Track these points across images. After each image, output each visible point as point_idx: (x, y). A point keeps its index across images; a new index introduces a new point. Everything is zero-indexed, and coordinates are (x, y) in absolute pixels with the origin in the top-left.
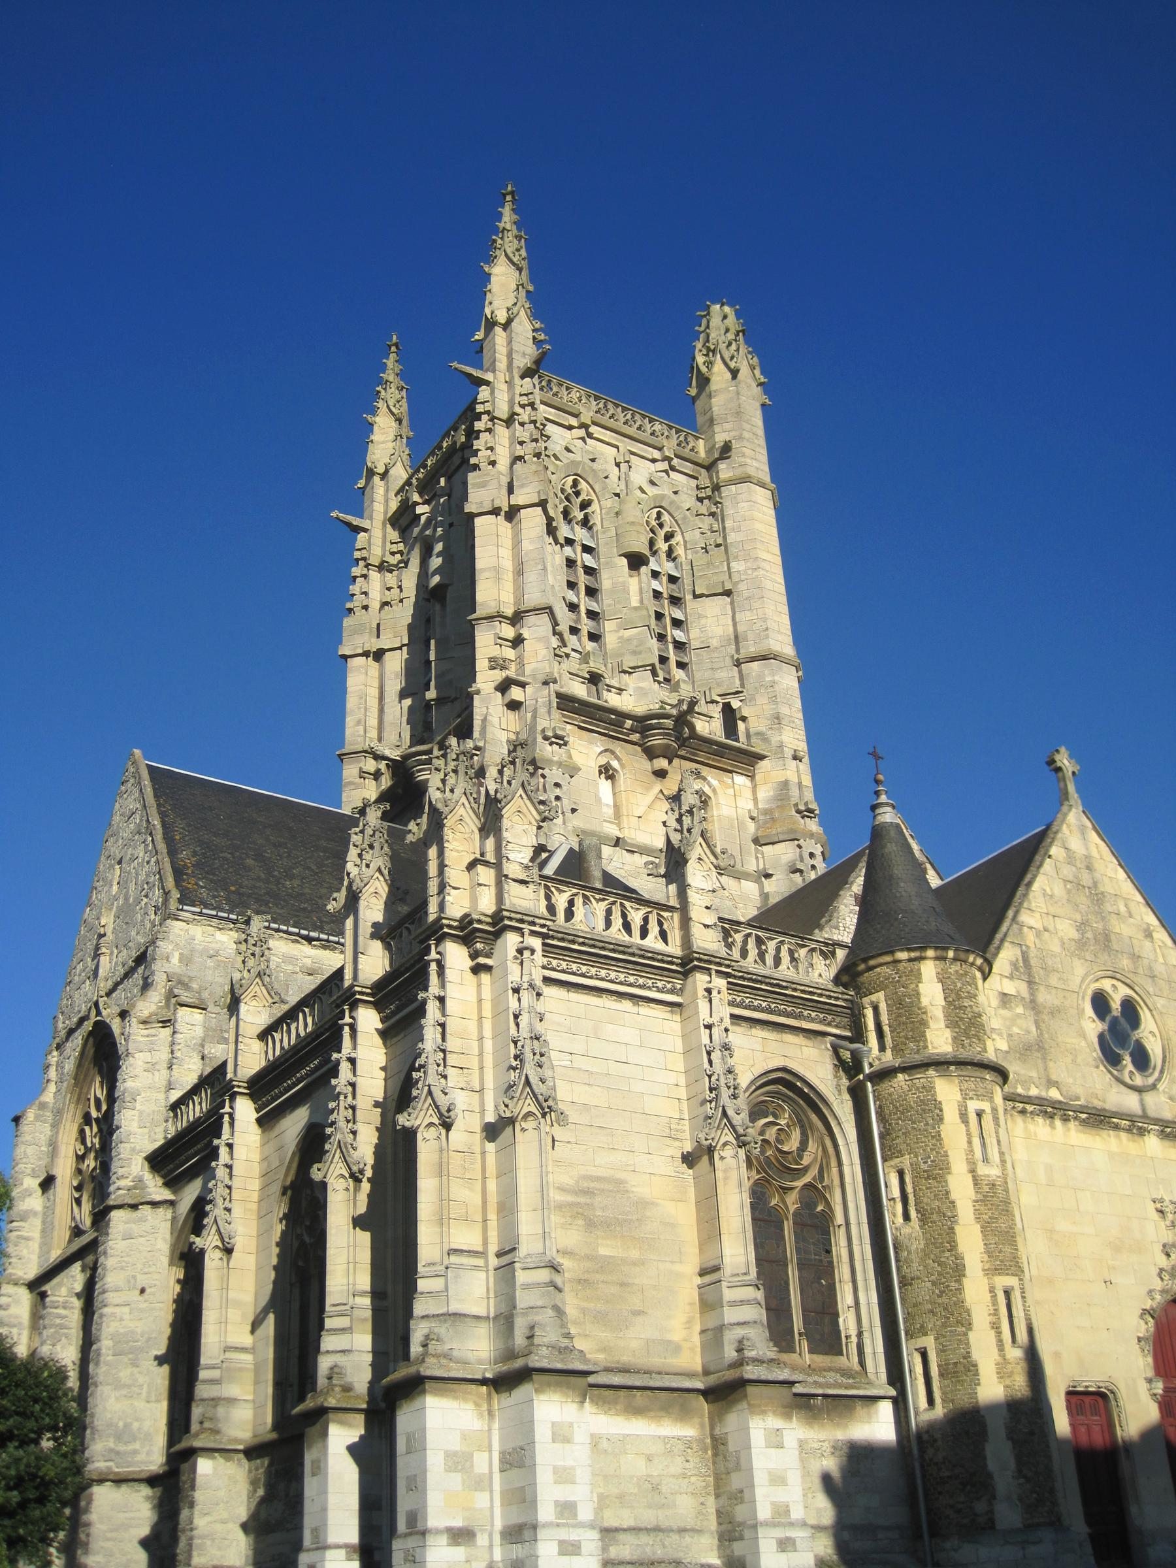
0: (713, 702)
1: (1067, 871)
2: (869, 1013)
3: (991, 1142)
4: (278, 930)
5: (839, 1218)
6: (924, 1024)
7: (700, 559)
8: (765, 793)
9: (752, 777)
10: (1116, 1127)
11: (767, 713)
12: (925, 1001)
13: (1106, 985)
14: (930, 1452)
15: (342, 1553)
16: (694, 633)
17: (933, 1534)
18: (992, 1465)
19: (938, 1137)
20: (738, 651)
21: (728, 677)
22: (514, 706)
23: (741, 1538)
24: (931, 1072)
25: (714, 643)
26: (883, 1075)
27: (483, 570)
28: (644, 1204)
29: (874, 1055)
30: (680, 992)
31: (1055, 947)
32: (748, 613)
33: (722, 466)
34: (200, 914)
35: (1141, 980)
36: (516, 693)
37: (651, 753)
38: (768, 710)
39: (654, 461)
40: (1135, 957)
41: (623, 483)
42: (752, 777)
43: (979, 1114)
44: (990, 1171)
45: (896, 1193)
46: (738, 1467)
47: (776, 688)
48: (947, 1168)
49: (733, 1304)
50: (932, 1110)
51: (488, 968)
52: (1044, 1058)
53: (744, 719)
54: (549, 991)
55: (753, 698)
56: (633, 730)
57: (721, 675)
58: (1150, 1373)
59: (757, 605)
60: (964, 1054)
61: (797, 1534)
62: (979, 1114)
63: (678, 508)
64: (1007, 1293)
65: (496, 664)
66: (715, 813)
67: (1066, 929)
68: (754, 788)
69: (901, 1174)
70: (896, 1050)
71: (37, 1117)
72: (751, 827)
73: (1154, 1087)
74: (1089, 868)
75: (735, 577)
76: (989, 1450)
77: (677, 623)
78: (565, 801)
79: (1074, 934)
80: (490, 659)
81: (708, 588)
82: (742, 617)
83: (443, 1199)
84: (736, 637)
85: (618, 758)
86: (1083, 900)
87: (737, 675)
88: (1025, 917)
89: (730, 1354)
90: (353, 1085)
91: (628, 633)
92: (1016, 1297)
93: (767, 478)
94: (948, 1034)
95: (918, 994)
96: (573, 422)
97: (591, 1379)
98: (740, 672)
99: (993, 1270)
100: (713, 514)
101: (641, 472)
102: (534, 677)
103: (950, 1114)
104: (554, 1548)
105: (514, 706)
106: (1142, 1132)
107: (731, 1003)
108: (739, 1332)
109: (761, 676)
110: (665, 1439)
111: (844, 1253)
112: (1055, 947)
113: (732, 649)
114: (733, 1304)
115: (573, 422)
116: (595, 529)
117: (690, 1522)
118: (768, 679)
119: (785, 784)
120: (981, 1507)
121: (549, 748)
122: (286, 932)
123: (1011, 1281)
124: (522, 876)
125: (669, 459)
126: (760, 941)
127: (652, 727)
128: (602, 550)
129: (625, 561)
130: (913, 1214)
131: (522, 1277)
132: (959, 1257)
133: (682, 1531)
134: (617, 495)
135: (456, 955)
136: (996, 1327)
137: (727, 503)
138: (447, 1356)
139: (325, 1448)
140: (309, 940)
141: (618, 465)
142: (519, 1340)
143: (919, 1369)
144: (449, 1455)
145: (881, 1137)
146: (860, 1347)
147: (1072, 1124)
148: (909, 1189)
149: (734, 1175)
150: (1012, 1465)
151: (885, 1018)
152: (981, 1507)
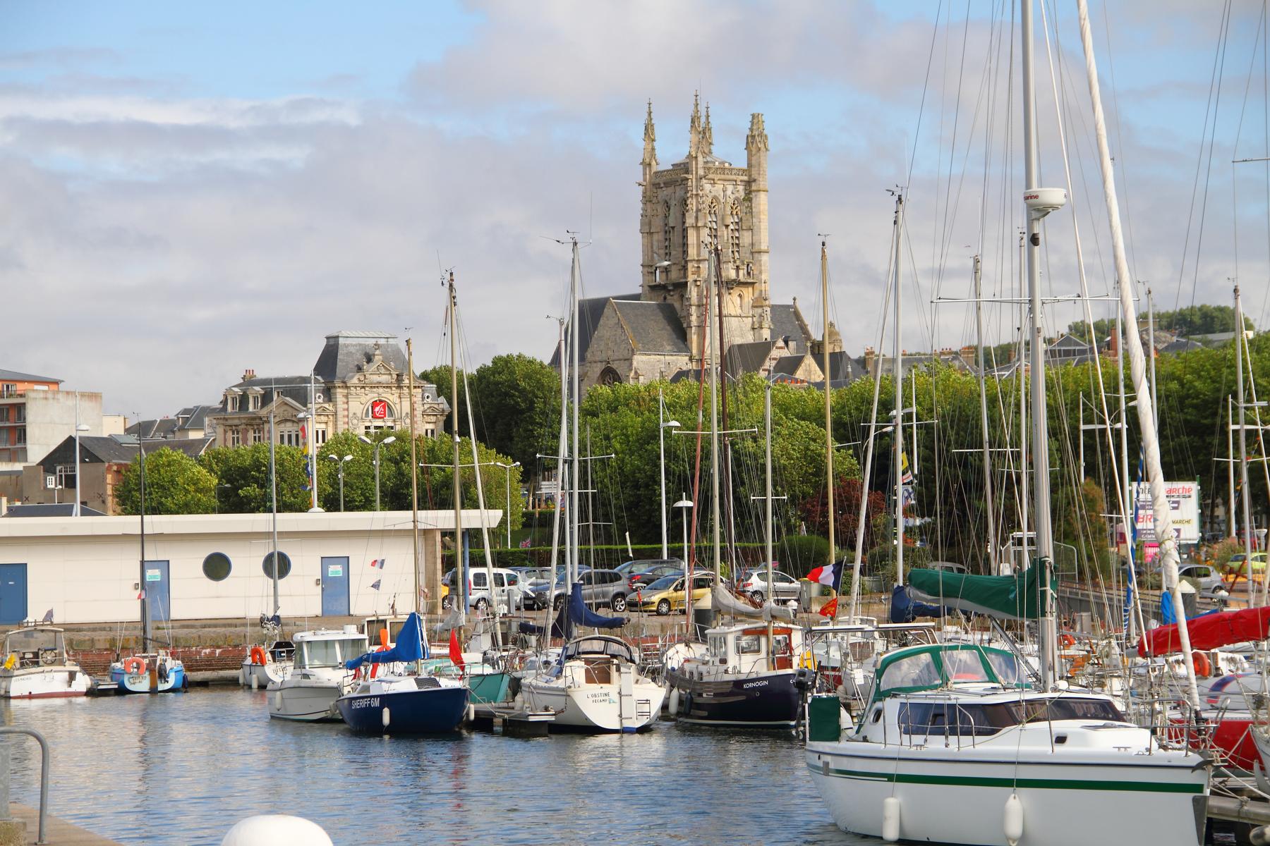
25: (746, 245)
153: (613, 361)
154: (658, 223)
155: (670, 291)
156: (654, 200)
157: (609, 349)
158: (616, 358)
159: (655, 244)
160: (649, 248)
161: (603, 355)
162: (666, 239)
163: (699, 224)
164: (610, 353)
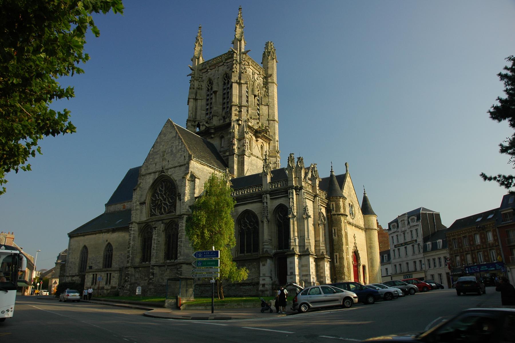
2: (331, 205)
6: (340, 208)
12: (340, 205)
15: (269, 277)
20: (269, 117)
23: (323, 278)
27: (234, 95)
34: (196, 160)
41: (254, 78)
75: (270, 103)
77: (258, 109)
80: (235, 114)
84: (268, 115)
90: (267, 207)
91: (253, 111)
93: (276, 83)
98: (269, 122)
103: (343, 222)
108: (323, 250)
109: (273, 124)
130: (336, 236)
136: (346, 253)
140: (210, 167)
148: (336, 232)
153: (168, 169)
155: (212, 133)
157: (164, 159)
158: (170, 166)
159: (199, 108)
160: (194, 110)
162: (207, 104)
163: (242, 82)
164: (165, 163)
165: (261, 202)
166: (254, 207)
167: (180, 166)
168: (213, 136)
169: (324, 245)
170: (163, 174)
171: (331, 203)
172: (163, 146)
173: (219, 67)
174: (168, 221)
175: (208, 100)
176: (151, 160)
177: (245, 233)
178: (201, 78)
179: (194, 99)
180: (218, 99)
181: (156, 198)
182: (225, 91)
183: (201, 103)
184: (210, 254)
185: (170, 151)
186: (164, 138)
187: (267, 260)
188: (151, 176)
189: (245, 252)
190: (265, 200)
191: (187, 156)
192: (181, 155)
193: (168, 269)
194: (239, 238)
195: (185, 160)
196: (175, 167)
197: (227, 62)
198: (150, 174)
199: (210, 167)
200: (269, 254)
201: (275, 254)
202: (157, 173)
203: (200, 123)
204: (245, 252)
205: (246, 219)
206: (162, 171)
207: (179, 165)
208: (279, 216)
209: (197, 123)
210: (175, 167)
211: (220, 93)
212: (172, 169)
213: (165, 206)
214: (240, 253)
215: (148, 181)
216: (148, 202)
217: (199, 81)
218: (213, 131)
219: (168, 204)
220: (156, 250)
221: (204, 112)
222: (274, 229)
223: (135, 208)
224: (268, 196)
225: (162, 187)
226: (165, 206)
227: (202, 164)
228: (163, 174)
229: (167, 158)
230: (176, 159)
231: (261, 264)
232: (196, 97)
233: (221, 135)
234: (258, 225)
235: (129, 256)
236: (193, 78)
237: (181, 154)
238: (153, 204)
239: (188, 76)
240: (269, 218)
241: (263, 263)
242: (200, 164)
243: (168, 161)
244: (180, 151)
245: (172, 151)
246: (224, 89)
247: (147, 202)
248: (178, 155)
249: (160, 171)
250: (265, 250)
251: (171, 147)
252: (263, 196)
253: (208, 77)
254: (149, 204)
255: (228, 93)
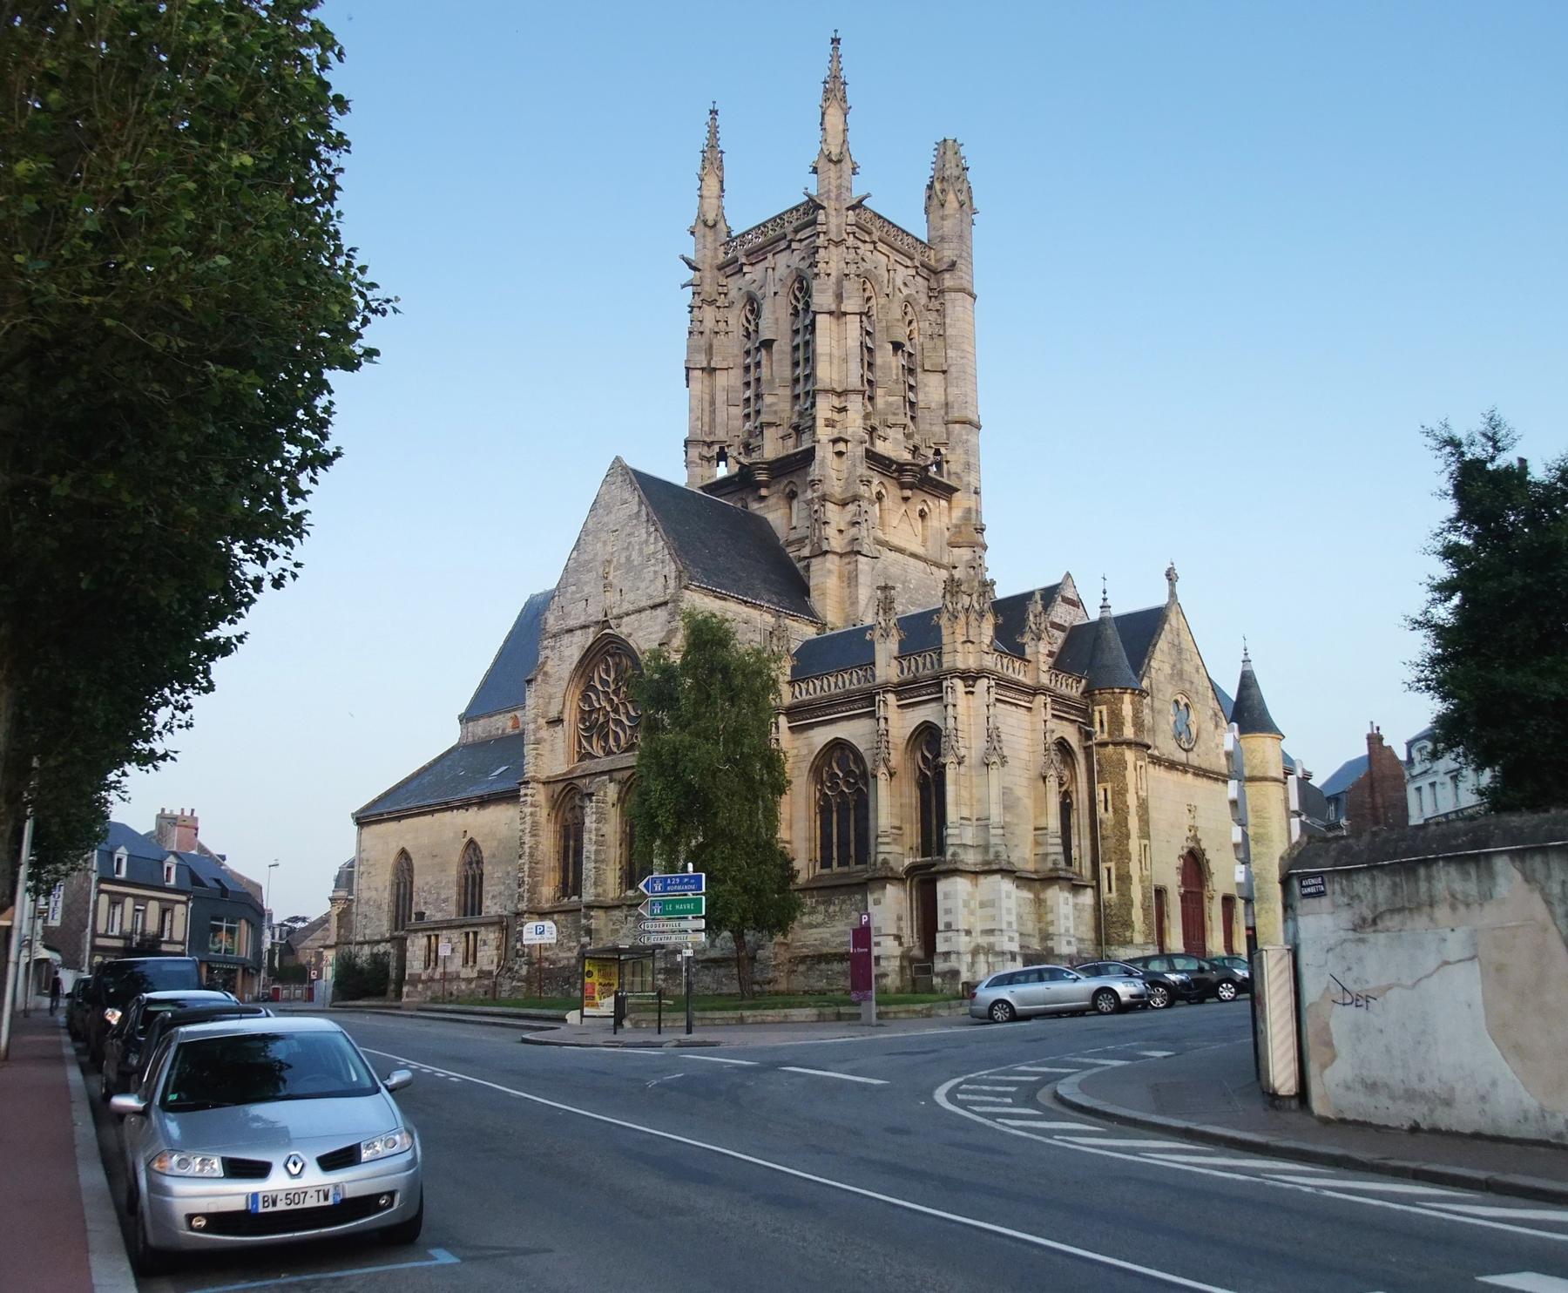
0: (930, 447)
1: (1170, 637)
3: (1144, 780)
4: (733, 597)
5: (1075, 807)
6: (1123, 724)
7: (928, 344)
8: (957, 514)
9: (949, 501)
10: (1178, 770)
11: (962, 461)
12: (1124, 713)
13: (1179, 697)
14: (1108, 911)
15: (892, 938)
16: (921, 396)
17: (1107, 944)
18: (1134, 918)
19: (1124, 776)
20: (946, 413)
21: (939, 429)
22: (840, 454)
23: (1052, 939)
24: (1124, 747)
25: (933, 405)
26: (1104, 744)
28: (1019, 799)
29: (1101, 735)
30: (1030, 702)
31: (1162, 679)
32: (955, 389)
33: (947, 275)
34: (699, 587)
35: (1191, 694)
36: (841, 447)
37: (903, 486)
38: (963, 458)
39: (907, 267)
40: (1192, 683)
41: (891, 285)
42: (949, 501)
43: (1141, 767)
44: (1143, 794)
45: (1103, 798)
46: (1052, 912)
47: (969, 444)
48: (1127, 791)
49: (1052, 845)
50: (1122, 764)
51: (972, 693)
52: (1154, 735)
53: (947, 462)
54: (998, 704)
55: (954, 449)
56: (895, 471)
57: (936, 429)
58: (1180, 883)
59: (962, 384)
60: (1138, 740)
61: (1072, 939)
62: (1141, 767)
63: (918, 303)
64: (1145, 846)
65: (830, 423)
66: (929, 524)
67: (1167, 669)
68: (950, 508)
69: (1105, 790)
70: (1110, 734)
71: (542, 681)
72: (947, 534)
73: (1192, 749)
74: (1178, 635)
75: (949, 361)
76: (1134, 912)
77: (911, 387)
78: (870, 522)
79: (1170, 672)
80: (826, 419)
81: (932, 366)
82: (952, 390)
83: (958, 795)
85: (885, 488)
86: (1174, 652)
87: (944, 430)
88: (1152, 663)
89: (1050, 865)
90: (887, 731)
91: (891, 399)
92: (1148, 848)
94: (1132, 730)
95: (1121, 709)
96: (867, 238)
97: (1017, 874)
98: (947, 429)
99: (1141, 837)
100: (937, 311)
101: (902, 274)
102: (853, 436)
103: (1130, 766)
104: (942, 940)
105: (840, 454)
106: (1186, 772)
107: (1053, 709)
108: (1054, 857)
110: (1024, 899)
111: (1076, 821)
112: (1162, 679)
113: (943, 412)
114: (1052, 845)
115: (867, 238)
116: (873, 318)
117: (1031, 932)
118: (965, 437)
119: (969, 510)
120: (1128, 934)
121: (862, 487)
122: (737, 598)
123: (1146, 842)
124: (986, 650)
125: (916, 267)
126: (1057, 676)
127: (907, 470)
128: (877, 335)
129: (891, 347)
130: (1110, 808)
131: (993, 831)
132: (1128, 830)
133: (1029, 935)
134: (888, 295)
135: (959, 684)
137: (948, 305)
138: (962, 861)
139: (884, 895)
140: (746, 602)
141: (889, 271)
142: (991, 857)
143: (1106, 875)
144: (964, 901)
145: (1098, 772)
146: (1080, 863)
147: (1162, 768)
148: (1109, 797)
149: (1053, 789)
150: (1142, 919)
151: (1105, 718)
152: (1128, 934)
153: (620, 617)
154: (731, 348)
155: (761, 485)
156: (721, 301)
157: (607, 587)
158: (626, 607)
159: (721, 398)
160: (706, 405)
161: (590, 610)
162: (747, 384)
164: (612, 597)
165: (872, 714)
166: (854, 731)
167: (654, 607)
168: (764, 492)
169: (1059, 841)
170: (607, 631)
171: (1096, 708)
172: (605, 543)
173: (776, 256)
174: (627, 773)
175: (747, 369)
176: (574, 588)
177: (834, 809)
178: (723, 296)
179: (703, 369)
180: (777, 367)
181: (591, 705)
182: (799, 340)
183: (730, 380)
184: (681, 883)
185: (623, 560)
186: (606, 519)
187: (885, 888)
188: (575, 639)
189: (835, 864)
190: (882, 713)
191: (673, 575)
192: (655, 572)
193: (630, 916)
194: (818, 823)
195: (666, 587)
196: (640, 611)
197: (798, 237)
198: (570, 631)
199: (746, 602)
200: (892, 869)
201: (912, 870)
202: (592, 629)
203: (726, 450)
204: (835, 864)
205: (834, 765)
206: (605, 624)
207: (650, 603)
208: (924, 757)
209: (716, 448)
210: (640, 611)
211: (783, 346)
212: (632, 617)
213: (618, 730)
214: (822, 867)
215: (567, 653)
216: (571, 716)
217: (718, 307)
218: (763, 478)
219: (626, 722)
220: (596, 862)
221: (738, 412)
222: (911, 795)
223: (532, 738)
224: (891, 698)
225: (608, 673)
226: (618, 730)
227: (720, 598)
228: (607, 631)
229: (615, 582)
230: (643, 585)
231: (870, 899)
232: (709, 363)
233: (787, 490)
234: (866, 785)
235: (523, 881)
236: (696, 296)
237: (657, 569)
238: (584, 724)
239: (684, 286)
240: (893, 763)
241: (876, 896)
242: (716, 597)
243: (621, 591)
244: (653, 561)
245: (628, 558)
246: (796, 332)
247: (566, 717)
248: (648, 573)
249: (597, 623)
250: (881, 857)
251: (627, 548)
252: (877, 698)
253: (744, 290)
254: (572, 723)
255: (807, 343)
